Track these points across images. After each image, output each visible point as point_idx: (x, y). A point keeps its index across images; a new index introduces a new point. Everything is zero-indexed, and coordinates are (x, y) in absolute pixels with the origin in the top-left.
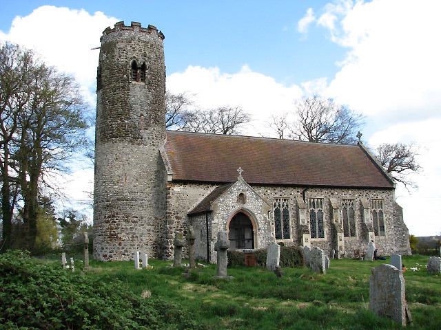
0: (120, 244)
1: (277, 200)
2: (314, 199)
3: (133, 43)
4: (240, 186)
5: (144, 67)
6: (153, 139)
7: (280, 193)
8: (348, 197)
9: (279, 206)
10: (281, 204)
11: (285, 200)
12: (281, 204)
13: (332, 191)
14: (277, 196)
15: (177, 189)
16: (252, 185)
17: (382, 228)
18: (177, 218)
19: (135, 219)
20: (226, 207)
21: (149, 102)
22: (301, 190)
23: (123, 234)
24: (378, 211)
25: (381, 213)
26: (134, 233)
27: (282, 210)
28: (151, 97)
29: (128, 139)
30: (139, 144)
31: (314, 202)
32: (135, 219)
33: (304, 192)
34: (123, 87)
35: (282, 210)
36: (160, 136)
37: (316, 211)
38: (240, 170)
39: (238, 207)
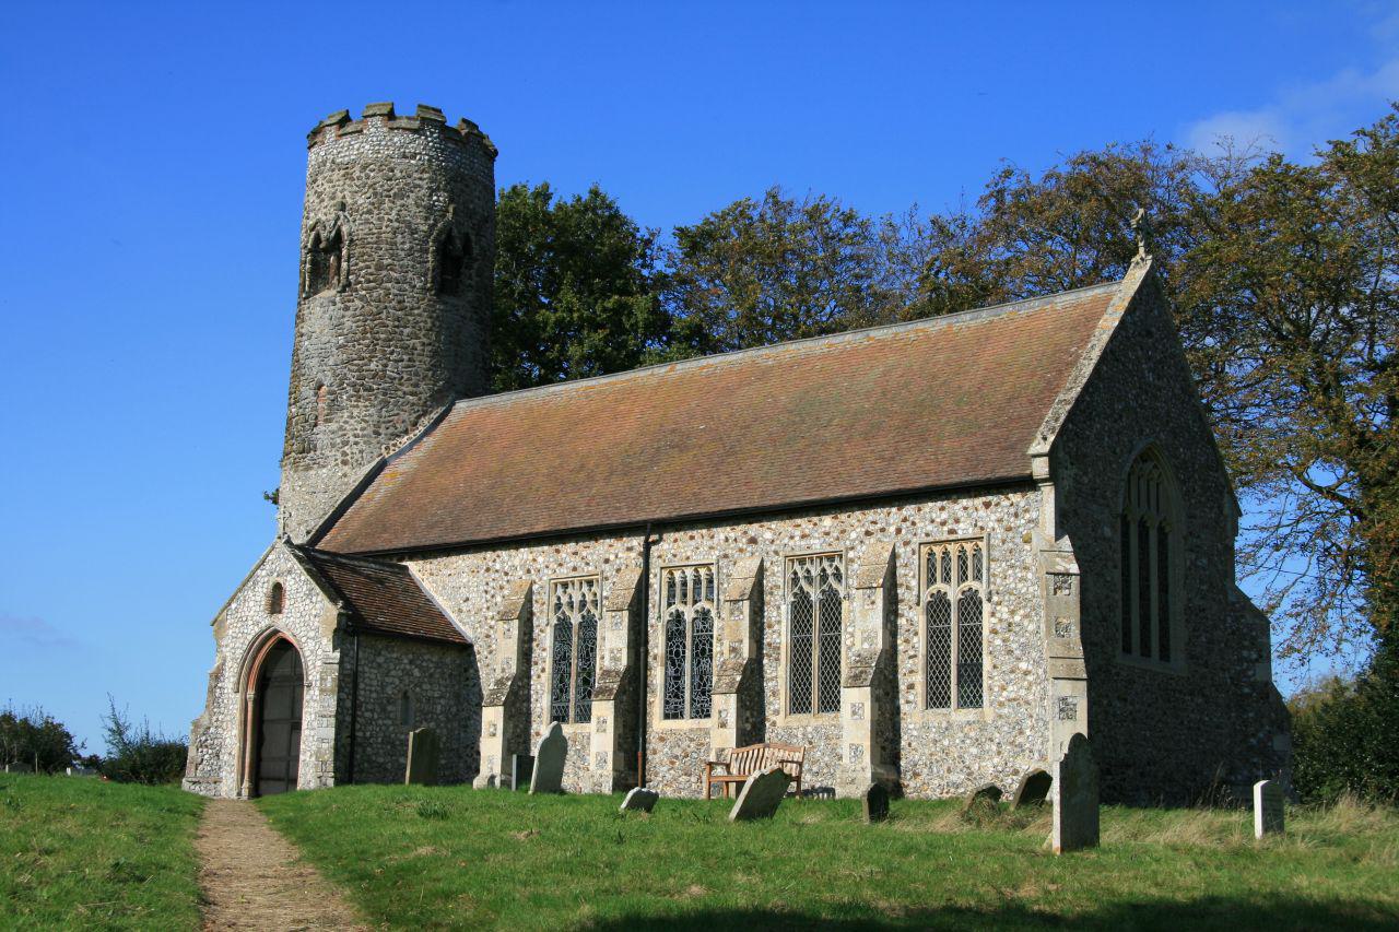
2: (697, 567)
6: (346, 443)
7: (576, 561)
8: (817, 545)
12: (577, 598)
13: (753, 529)
14: (564, 572)
17: (971, 674)
21: (341, 340)
22: (637, 542)
24: (953, 593)
25: (971, 605)
28: (348, 323)
30: (308, 468)
33: (646, 555)
36: (369, 431)
37: (689, 613)
39: (266, 621)
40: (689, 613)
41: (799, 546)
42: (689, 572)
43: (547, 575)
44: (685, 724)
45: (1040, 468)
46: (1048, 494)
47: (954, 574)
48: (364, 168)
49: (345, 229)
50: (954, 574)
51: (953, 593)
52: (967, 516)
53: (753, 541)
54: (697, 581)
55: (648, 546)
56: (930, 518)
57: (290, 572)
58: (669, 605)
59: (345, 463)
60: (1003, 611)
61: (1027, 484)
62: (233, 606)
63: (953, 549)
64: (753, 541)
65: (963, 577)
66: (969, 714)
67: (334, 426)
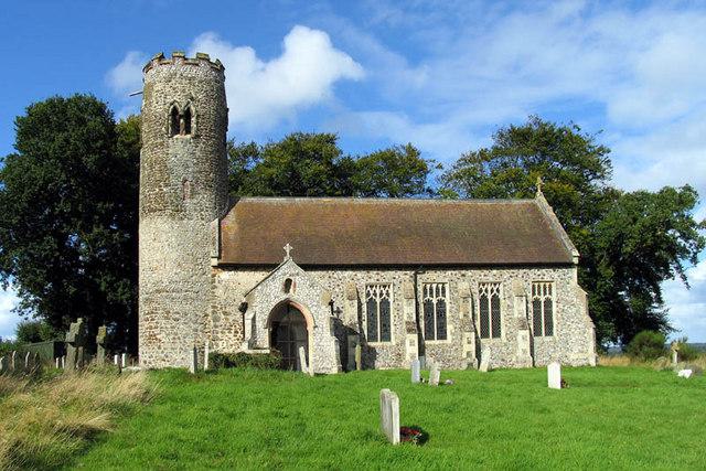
0: (159, 348)
1: (372, 287)
2: (431, 284)
3: (173, 81)
4: (289, 268)
5: (188, 115)
8: (491, 279)
9: (375, 295)
10: (378, 292)
11: (385, 286)
12: (378, 292)
13: (463, 272)
14: (372, 281)
15: (225, 275)
16: (306, 267)
18: (225, 313)
19: (177, 316)
20: (269, 294)
23: (163, 334)
24: (542, 299)
25: (548, 303)
26: (176, 334)
27: (378, 300)
29: (168, 212)
31: (431, 289)
32: (177, 316)
34: (162, 144)
35: (378, 300)
37: (435, 301)
38: (288, 248)
39: (284, 297)
40: (435, 301)
41: (484, 279)
42: (434, 286)
43: (363, 282)
44: (436, 342)
45: (576, 261)
46: (574, 272)
47: (542, 292)
48: (201, 82)
49: (193, 108)
50: (542, 292)
51: (542, 299)
52: (548, 274)
53: (463, 275)
54: (437, 288)
55: (415, 275)
56: (534, 274)
57: (297, 274)
58: (424, 297)
59: (202, 219)
60: (561, 306)
61: (569, 265)
62: (259, 288)
63: (542, 284)
64: (463, 275)
65: (545, 294)
66: (548, 339)
67: (195, 201)
